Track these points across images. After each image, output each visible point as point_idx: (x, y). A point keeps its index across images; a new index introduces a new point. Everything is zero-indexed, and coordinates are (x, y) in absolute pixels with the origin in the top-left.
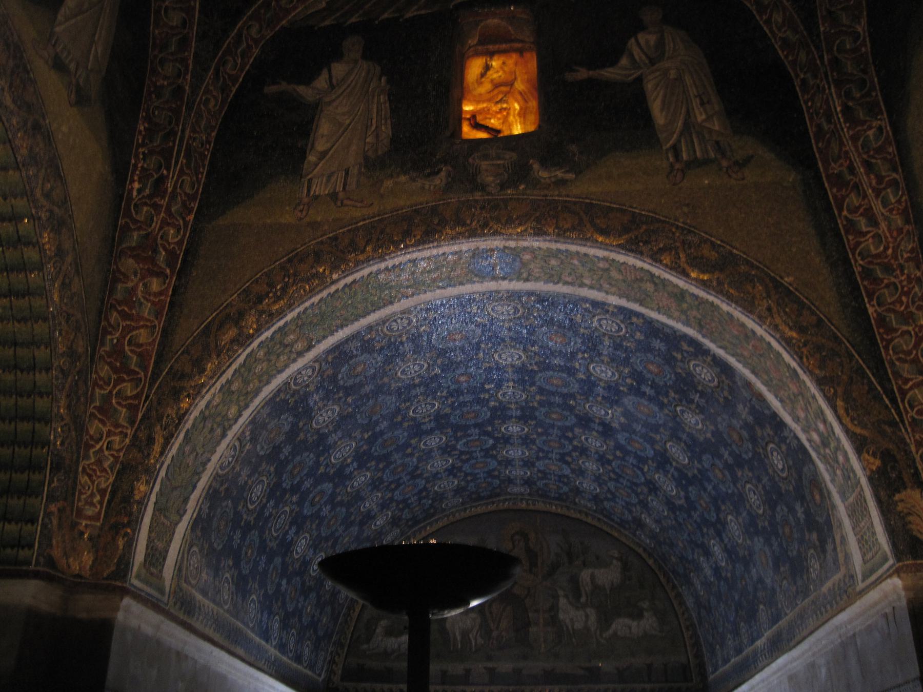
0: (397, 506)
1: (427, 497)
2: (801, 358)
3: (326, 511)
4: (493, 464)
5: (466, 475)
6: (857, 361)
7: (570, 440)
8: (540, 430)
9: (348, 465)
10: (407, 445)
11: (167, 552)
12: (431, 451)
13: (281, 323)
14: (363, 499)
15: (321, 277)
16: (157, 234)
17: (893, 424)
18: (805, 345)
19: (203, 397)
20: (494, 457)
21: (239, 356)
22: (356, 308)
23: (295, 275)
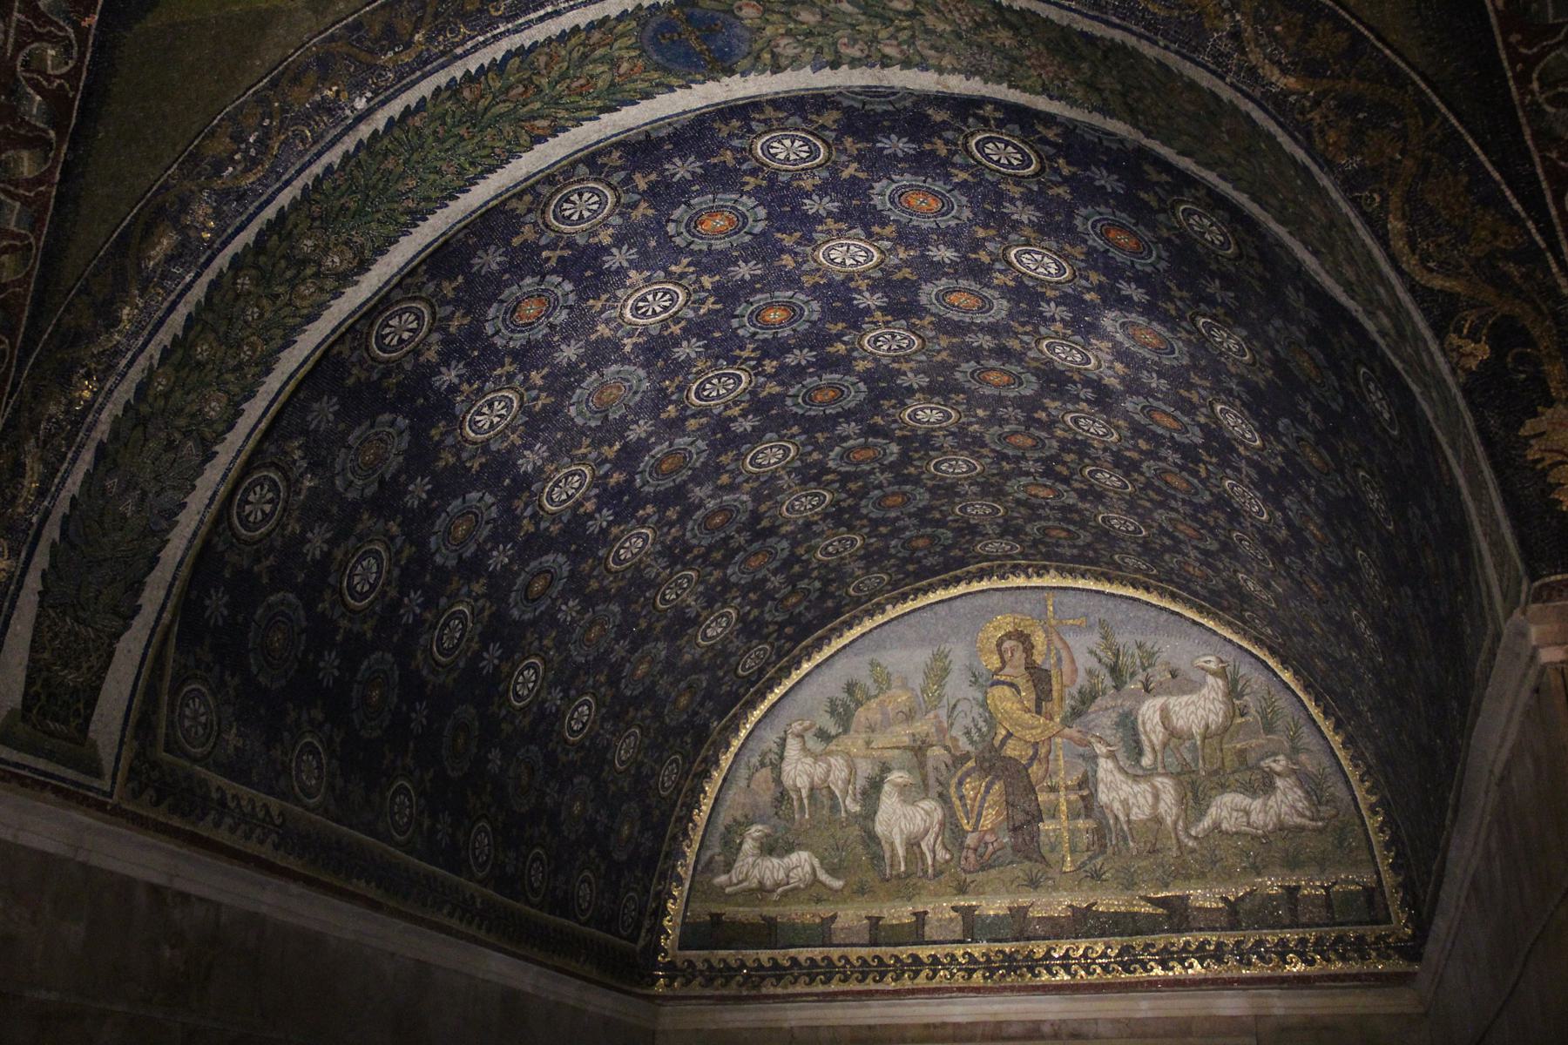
3: (569, 609)
4: (922, 498)
5: (875, 523)
6: (1446, 120)
8: (980, 413)
10: (709, 472)
11: (96, 690)
12: (773, 477)
13: (270, 212)
14: (654, 584)
15: (329, 108)
16: (14, 57)
17: (1528, 255)
18: (1317, 103)
19: (123, 375)
20: (916, 481)
21: (189, 287)
22: (438, 172)
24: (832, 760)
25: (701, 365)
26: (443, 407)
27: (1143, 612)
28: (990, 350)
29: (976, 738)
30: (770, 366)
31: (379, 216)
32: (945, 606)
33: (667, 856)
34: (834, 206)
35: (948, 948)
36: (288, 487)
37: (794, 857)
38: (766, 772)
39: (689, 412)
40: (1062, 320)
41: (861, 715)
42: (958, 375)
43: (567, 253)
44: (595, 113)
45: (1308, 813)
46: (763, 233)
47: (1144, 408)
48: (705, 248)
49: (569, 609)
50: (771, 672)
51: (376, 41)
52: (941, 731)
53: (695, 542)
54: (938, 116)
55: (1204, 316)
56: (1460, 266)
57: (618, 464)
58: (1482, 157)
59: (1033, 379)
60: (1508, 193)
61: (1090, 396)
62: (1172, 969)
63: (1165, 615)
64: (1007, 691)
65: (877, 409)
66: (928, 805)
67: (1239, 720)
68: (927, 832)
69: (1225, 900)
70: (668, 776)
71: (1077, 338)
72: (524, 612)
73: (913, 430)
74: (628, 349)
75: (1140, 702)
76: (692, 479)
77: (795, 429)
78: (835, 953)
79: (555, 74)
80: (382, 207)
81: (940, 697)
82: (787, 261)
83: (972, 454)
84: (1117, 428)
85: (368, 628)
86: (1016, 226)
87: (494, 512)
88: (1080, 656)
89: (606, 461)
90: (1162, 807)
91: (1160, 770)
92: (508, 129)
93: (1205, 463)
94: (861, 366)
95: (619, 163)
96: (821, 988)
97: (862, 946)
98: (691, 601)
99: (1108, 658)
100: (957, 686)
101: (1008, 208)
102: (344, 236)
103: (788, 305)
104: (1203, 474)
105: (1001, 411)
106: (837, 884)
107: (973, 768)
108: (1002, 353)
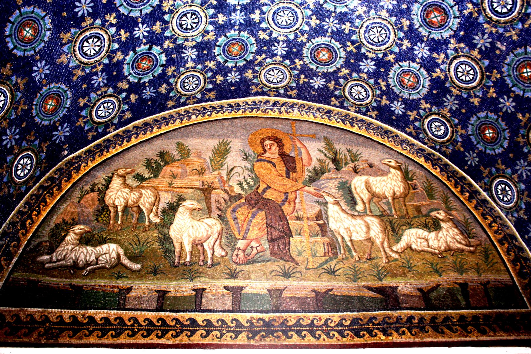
24: (143, 191)
27: (349, 136)
29: (246, 187)
32: (229, 122)
37: (105, 247)
41: (167, 169)
45: (463, 242)
62: (391, 335)
63: (362, 139)
67: (413, 191)
69: (420, 290)
75: (352, 178)
78: (126, 314)
88: (313, 152)
96: (111, 341)
106: (137, 266)
107: (244, 204)
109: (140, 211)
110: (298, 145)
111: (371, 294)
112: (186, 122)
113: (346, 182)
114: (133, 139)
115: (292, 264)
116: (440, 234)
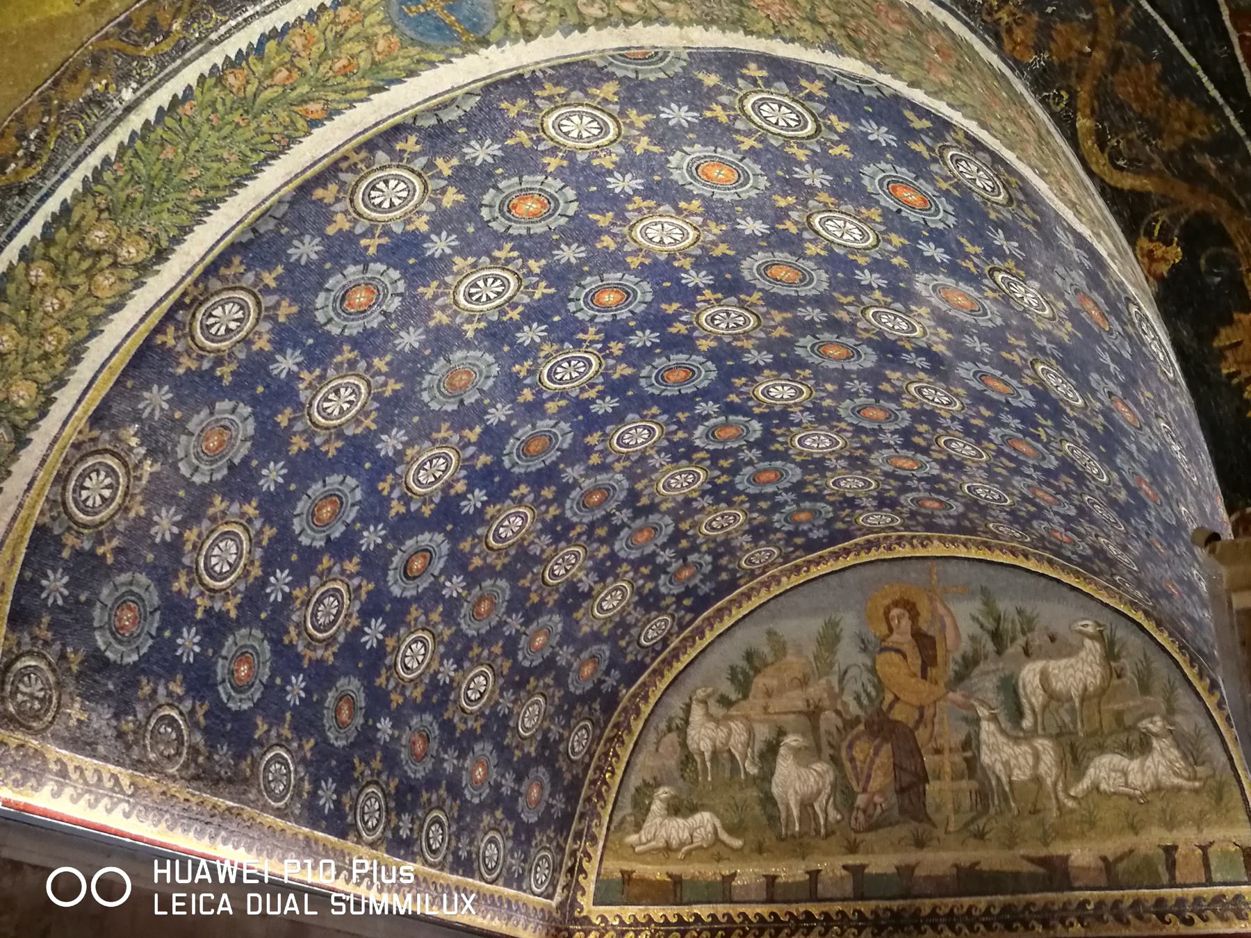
0: (636, 571)
1: (695, 548)
2: (997, 37)
4: (795, 474)
5: (754, 499)
7: (896, 397)
8: (830, 387)
9: (462, 496)
10: (578, 452)
12: (643, 458)
13: (53, 205)
15: (97, 101)
20: (784, 456)
22: (220, 159)
23: (61, 107)
25: (547, 349)
26: (284, 393)
28: (822, 323)
29: (865, 702)
30: (616, 348)
31: (169, 205)
32: (835, 578)
33: (582, 816)
34: (638, 183)
35: (838, 907)
36: (128, 473)
37: (698, 817)
38: (673, 737)
39: (545, 396)
40: (880, 287)
41: (760, 682)
42: (799, 351)
43: (385, 240)
44: (364, 94)
45: (1185, 774)
46: (576, 214)
47: (975, 374)
48: (524, 232)
49: (454, 586)
50: (674, 643)
51: (141, 34)
52: (834, 697)
53: (575, 519)
54: (711, 80)
55: (1000, 270)
56: (1151, 161)
57: (481, 445)
58: (1177, 43)
59: (870, 350)
60: (1205, 79)
61: (926, 365)
63: (1044, 581)
64: (896, 657)
65: (732, 389)
66: (819, 767)
67: (1116, 682)
68: (819, 793)
69: (1104, 859)
70: (578, 741)
71: (898, 306)
72: (404, 590)
73: (769, 406)
74: (470, 334)
76: (560, 459)
77: (655, 410)
79: (315, 56)
80: (169, 197)
81: (831, 665)
82: (607, 241)
83: (832, 428)
84: (957, 396)
85: (231, 607)
86: (812, 191)
87: (358, 495)
88: (962, 622)
89: (469, 444)
90: (1043, 769)
91: (1040, 731)
92: (283, 116)
93: (1043, 426)
94: (704, 345)
95: (418, 148)
97: (757, 902)
98: (581, 575)
99: (990, 625)
100: (848, 654)
101: (799, 174)
102: (136, 228)
103: (618, 287)
104: (1044, 437)
105: (849, 385)
106: (737, 843)
108: (834, 325)
109: (732, 757)
110: (941, 610)
111: (1031, 868)
112: (775, 590)
113: (1011, 676)
114: (707, 633)
115: (927, 826)
116: (1149, 763)
